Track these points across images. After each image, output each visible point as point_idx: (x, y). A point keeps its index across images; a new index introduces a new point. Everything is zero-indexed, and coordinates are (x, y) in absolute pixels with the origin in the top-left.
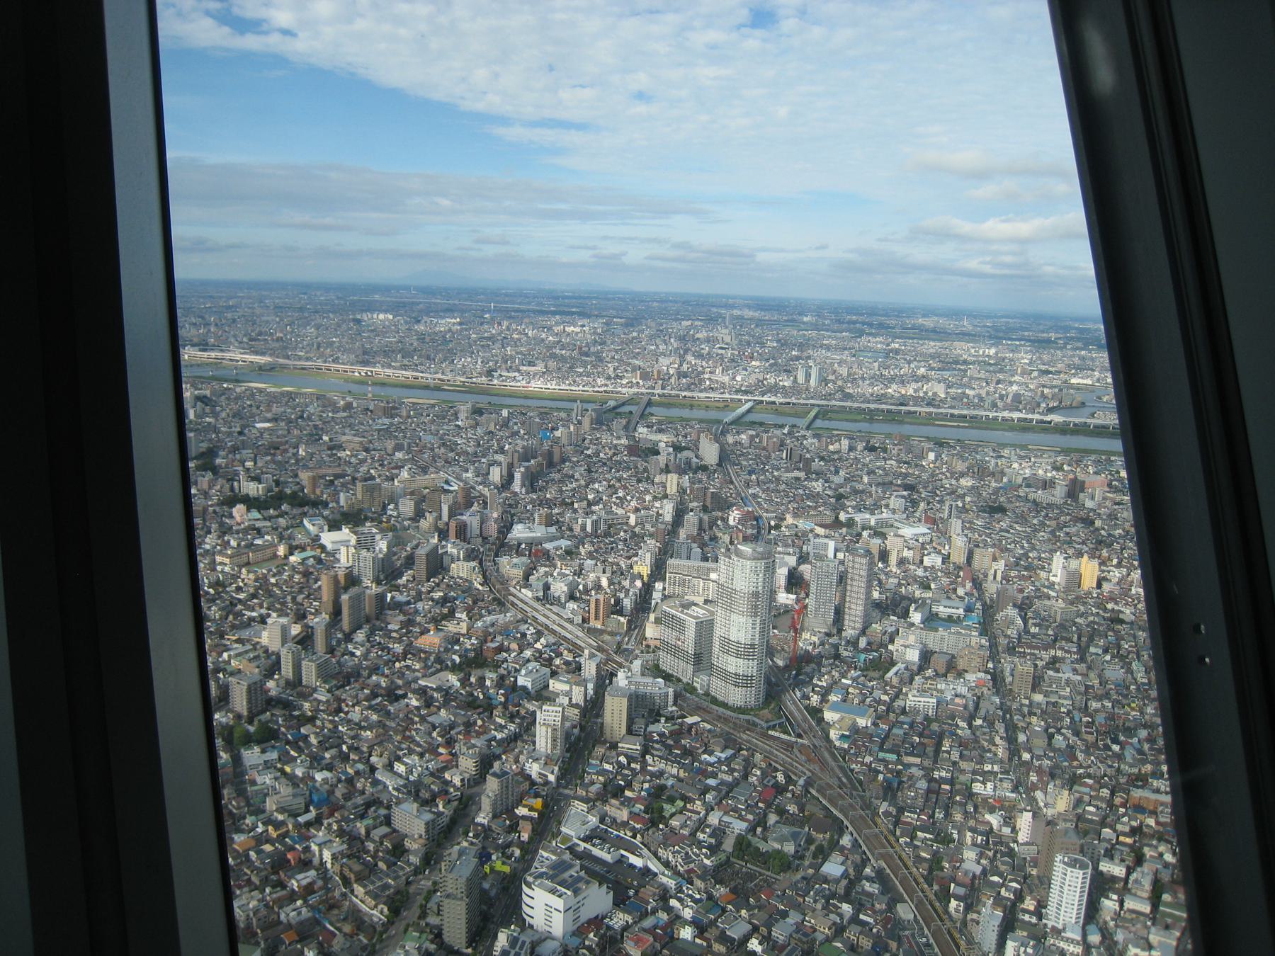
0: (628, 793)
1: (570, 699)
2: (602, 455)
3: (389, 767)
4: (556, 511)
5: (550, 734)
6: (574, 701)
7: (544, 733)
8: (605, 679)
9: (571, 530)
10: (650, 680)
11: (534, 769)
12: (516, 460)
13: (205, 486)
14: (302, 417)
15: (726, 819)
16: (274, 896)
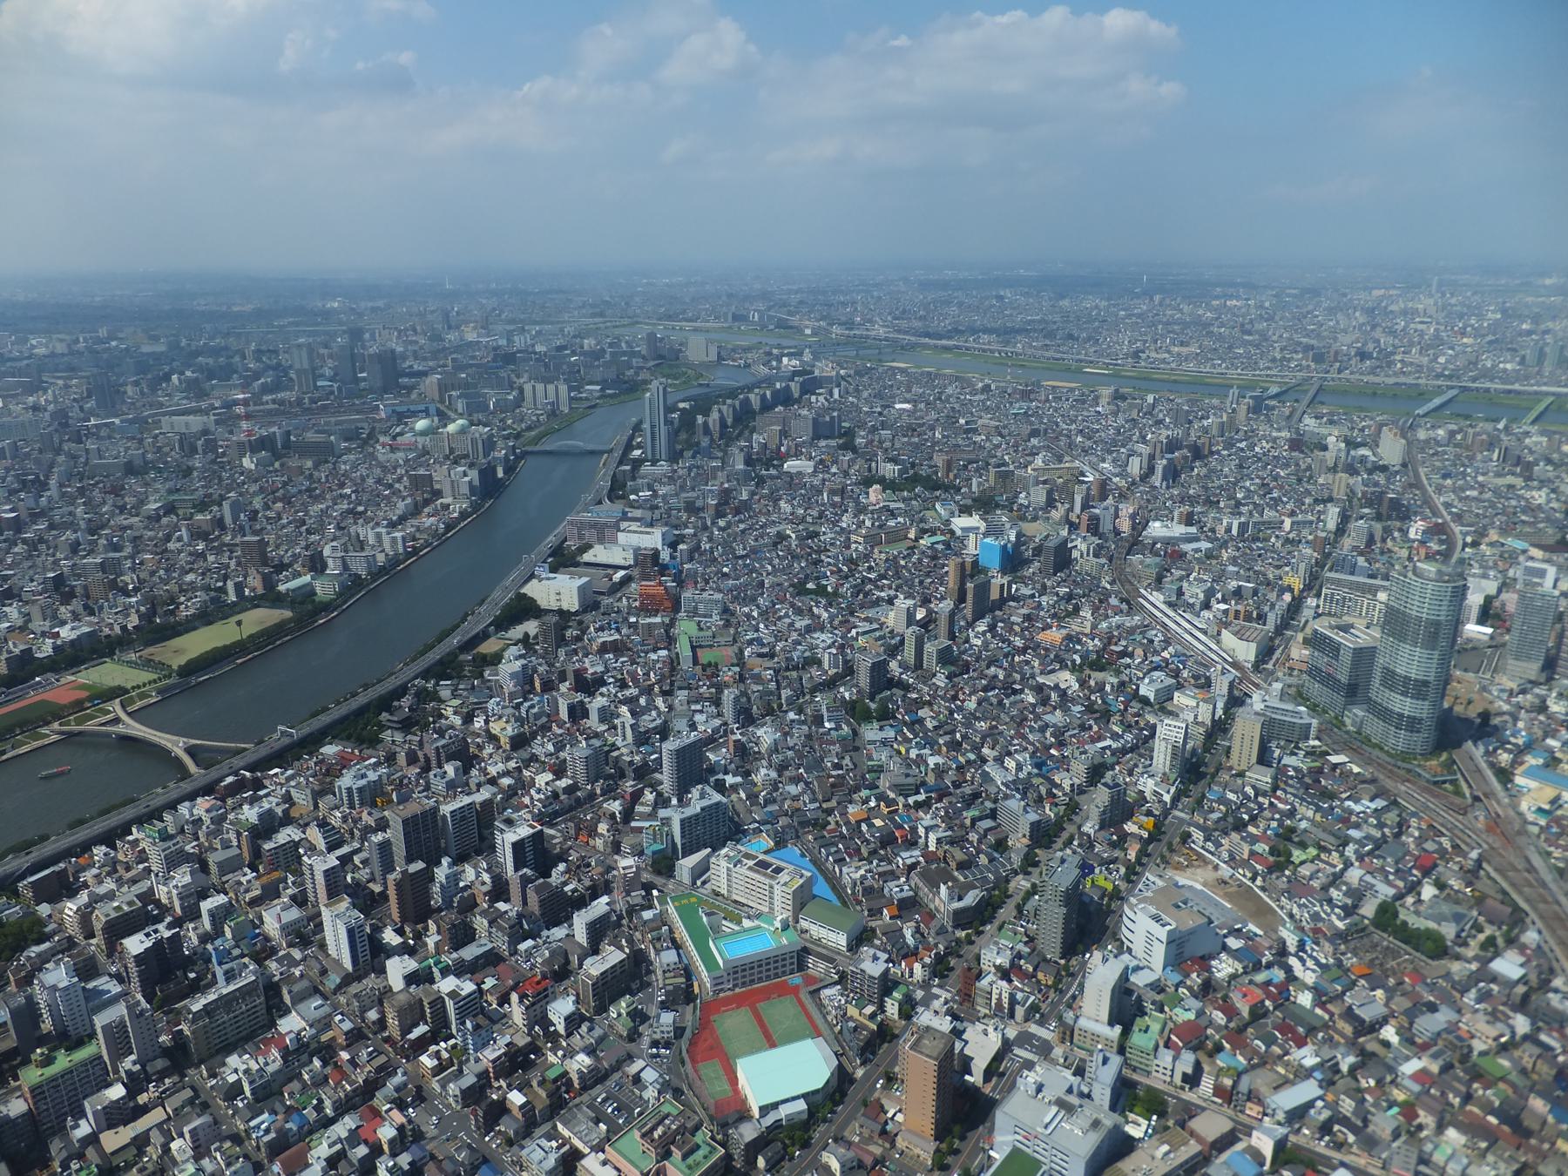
0: (1251, 829)
1: (1196, 717)
2: (1257, 449)
3: (999, 760)
4: (1198, 509)
5: (1169, 751)
6: (1200, 719)
7: (1163, 749)
8: (1236, 701)
9: (1213, 530)
10: (1290, 707)
11: (1148, 785)
12: (1158, 450)
13: (845, 466)
14: (940, 399)
15: (1368, 878)
16: (880, 869)
